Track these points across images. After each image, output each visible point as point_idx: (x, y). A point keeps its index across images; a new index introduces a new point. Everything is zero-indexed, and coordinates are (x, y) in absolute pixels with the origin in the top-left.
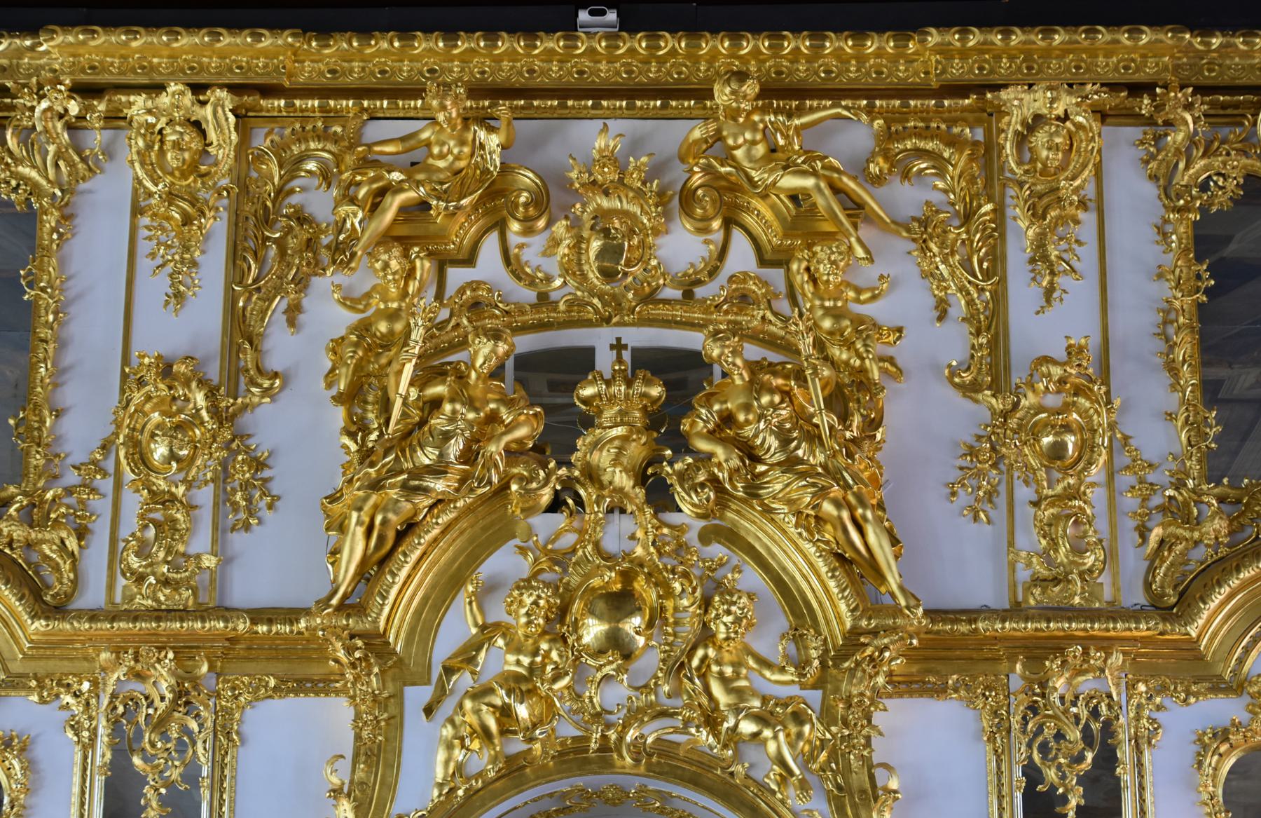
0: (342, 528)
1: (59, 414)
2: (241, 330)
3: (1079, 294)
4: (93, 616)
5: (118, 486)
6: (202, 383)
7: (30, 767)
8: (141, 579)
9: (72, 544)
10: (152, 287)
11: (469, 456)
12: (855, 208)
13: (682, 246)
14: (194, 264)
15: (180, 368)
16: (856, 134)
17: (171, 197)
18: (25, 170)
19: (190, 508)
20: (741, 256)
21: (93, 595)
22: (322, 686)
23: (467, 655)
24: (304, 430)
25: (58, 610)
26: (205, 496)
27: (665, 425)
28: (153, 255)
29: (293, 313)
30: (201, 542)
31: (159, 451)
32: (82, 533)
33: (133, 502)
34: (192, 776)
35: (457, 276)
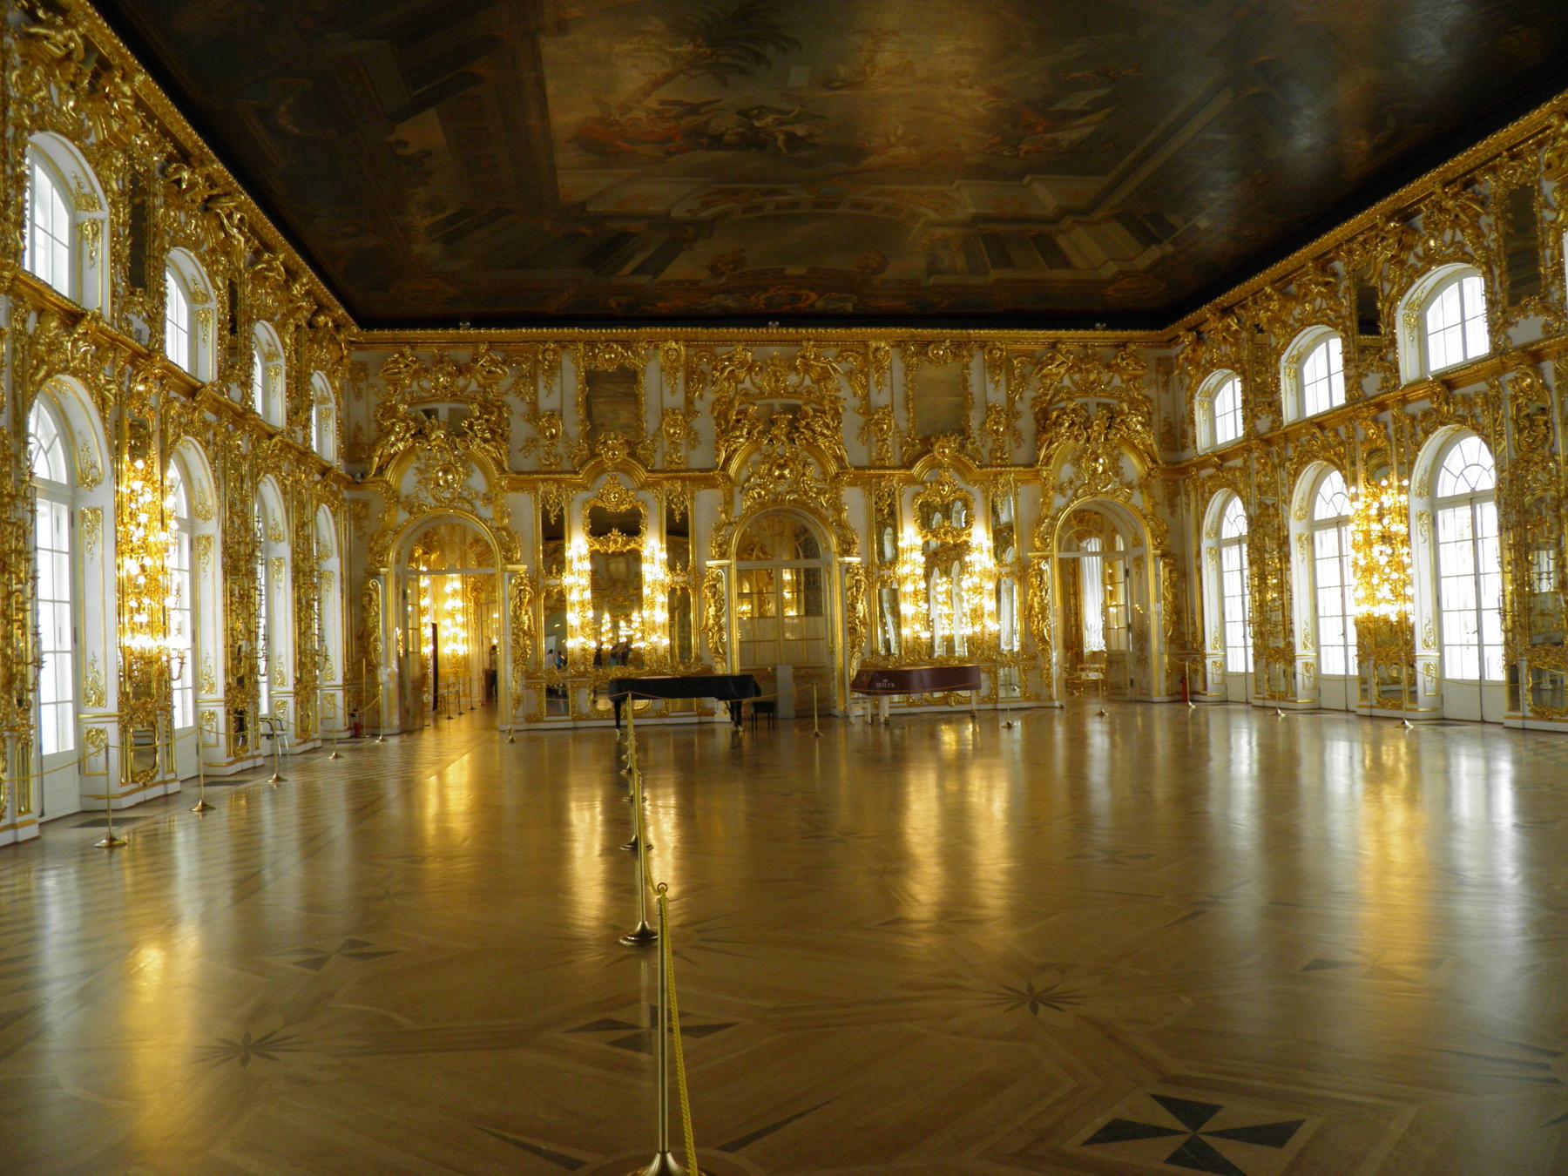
0: (719, 450)
2: (689, 402)
3: (886, 390)
10: (667, 390)
11: (749, 433)
12: (835, 370)
13: (793, 379)
20: (808, 381)
22: (714, 486)
23: (748, 480)
24: (705, 424)
25: (652, 471)
27: (793, 426)
29: (701, 396)
33: (666, 442)
35: (740, 386)
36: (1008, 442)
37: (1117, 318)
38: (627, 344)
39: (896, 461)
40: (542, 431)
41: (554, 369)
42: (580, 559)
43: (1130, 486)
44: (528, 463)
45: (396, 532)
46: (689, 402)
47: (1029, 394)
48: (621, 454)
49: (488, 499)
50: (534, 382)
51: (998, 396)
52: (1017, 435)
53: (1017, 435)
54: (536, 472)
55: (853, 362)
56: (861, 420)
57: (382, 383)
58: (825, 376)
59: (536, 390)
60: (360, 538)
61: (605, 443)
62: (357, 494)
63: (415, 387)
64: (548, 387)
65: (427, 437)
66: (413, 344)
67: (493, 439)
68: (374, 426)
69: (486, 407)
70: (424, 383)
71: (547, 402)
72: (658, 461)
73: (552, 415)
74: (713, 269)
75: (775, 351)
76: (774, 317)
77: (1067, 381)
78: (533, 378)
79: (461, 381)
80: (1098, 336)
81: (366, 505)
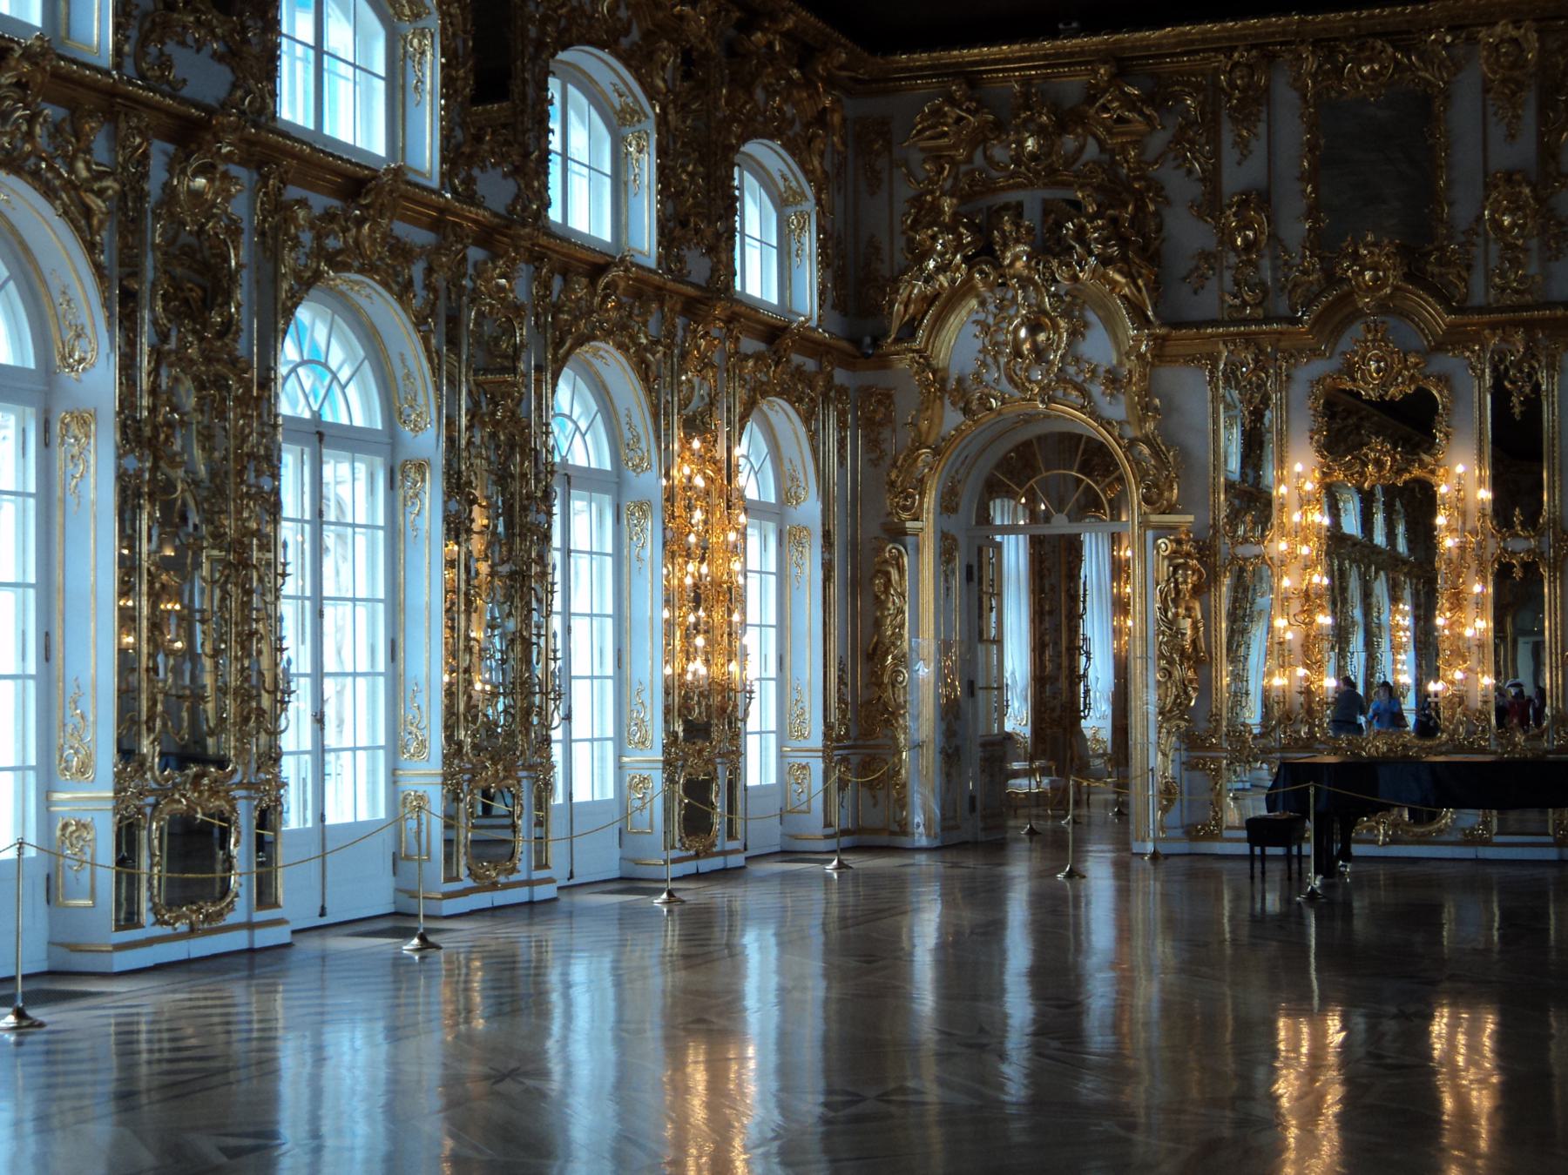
1: (1450, 204)
4: (1480, 310)
5: (1487, 241)
6: (1529, 184)
7: (1450, 389)
8: (1503, 290)
9: (1464, 274)
14: (1518, 117)
15: (1518, 177)
17: (1504, 81)
18: (1422, 74)
19: (1526, 250)
21: (1478, 298)
25: (1460, 310)
26: (1534, 243)
28: (1495, 114)
30: (1533, 268)
31: (1507, 221)
32: (1469, 268)
33: (1494, 249)
34: (1537, 386)
38: (1402, 38)
40: (1226, 238)
41: (1254, 103)
42: (1304, 502)
45: (937, 452)
49: (1114, 381)
54: (1214, 323)
57: (916, 157)
59: (1216, 153)
60: (875, 463)
61: (1356, 252)
62: (868, 377)
63: (978, 157)
64: (1243, 145)
65: (997, 264)
66: (971, 77)
67: (1124, 258)
68: (901, 242)
69: (1113, 191)
70: (999, 153)
71: (1237, 176)
73: (1244, 204)
79: (1069, 142)
81: (886, 398)
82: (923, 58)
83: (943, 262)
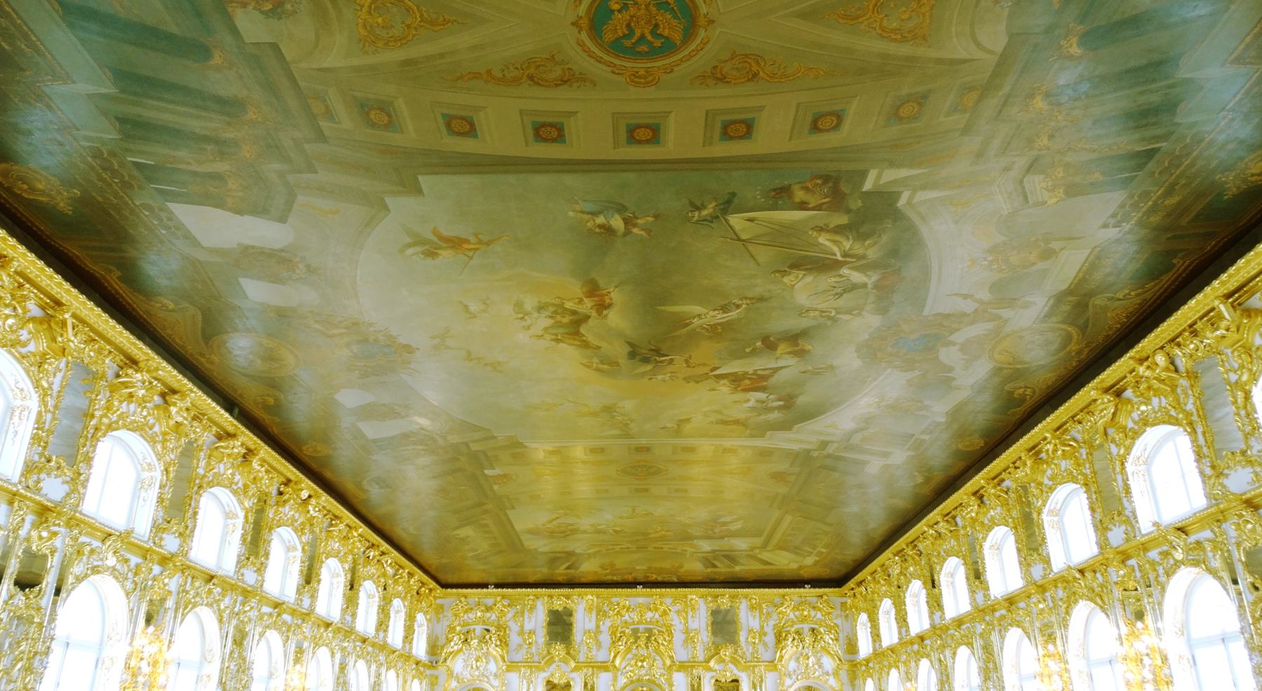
2: (598, 627)
13: (650, 615)
16: (668, 601)
20: (657, 616)
24: (605, 638)
27: (648, 638)
36: (761, 648)
37: (817, 583)
38: (568, 597)
39: (701, 659)
41: (532, 609)
43: (827, 674)
44: (519, 656)
46: (598, 627)
47: (772, 623)
48: (563, 653)
49: (496, 675)
50: (523, 615)
51: (755, 623)
52: (765, 645)
53: (765, 645)
55: (678, 607)
56: (683, 637)
58: (665, 613)
69: (499, 628)
71: (528, 627)
72: (582, 658)
74: (602, 567)
75: (641, 600)
76: (640, 584)
77: (792, 616)
78: (523, 613)
79: (488, 615)
80: (808, 591)
81: (437, 678)
82: (454, 590)
83: (456, 644)
